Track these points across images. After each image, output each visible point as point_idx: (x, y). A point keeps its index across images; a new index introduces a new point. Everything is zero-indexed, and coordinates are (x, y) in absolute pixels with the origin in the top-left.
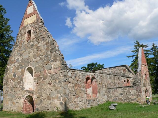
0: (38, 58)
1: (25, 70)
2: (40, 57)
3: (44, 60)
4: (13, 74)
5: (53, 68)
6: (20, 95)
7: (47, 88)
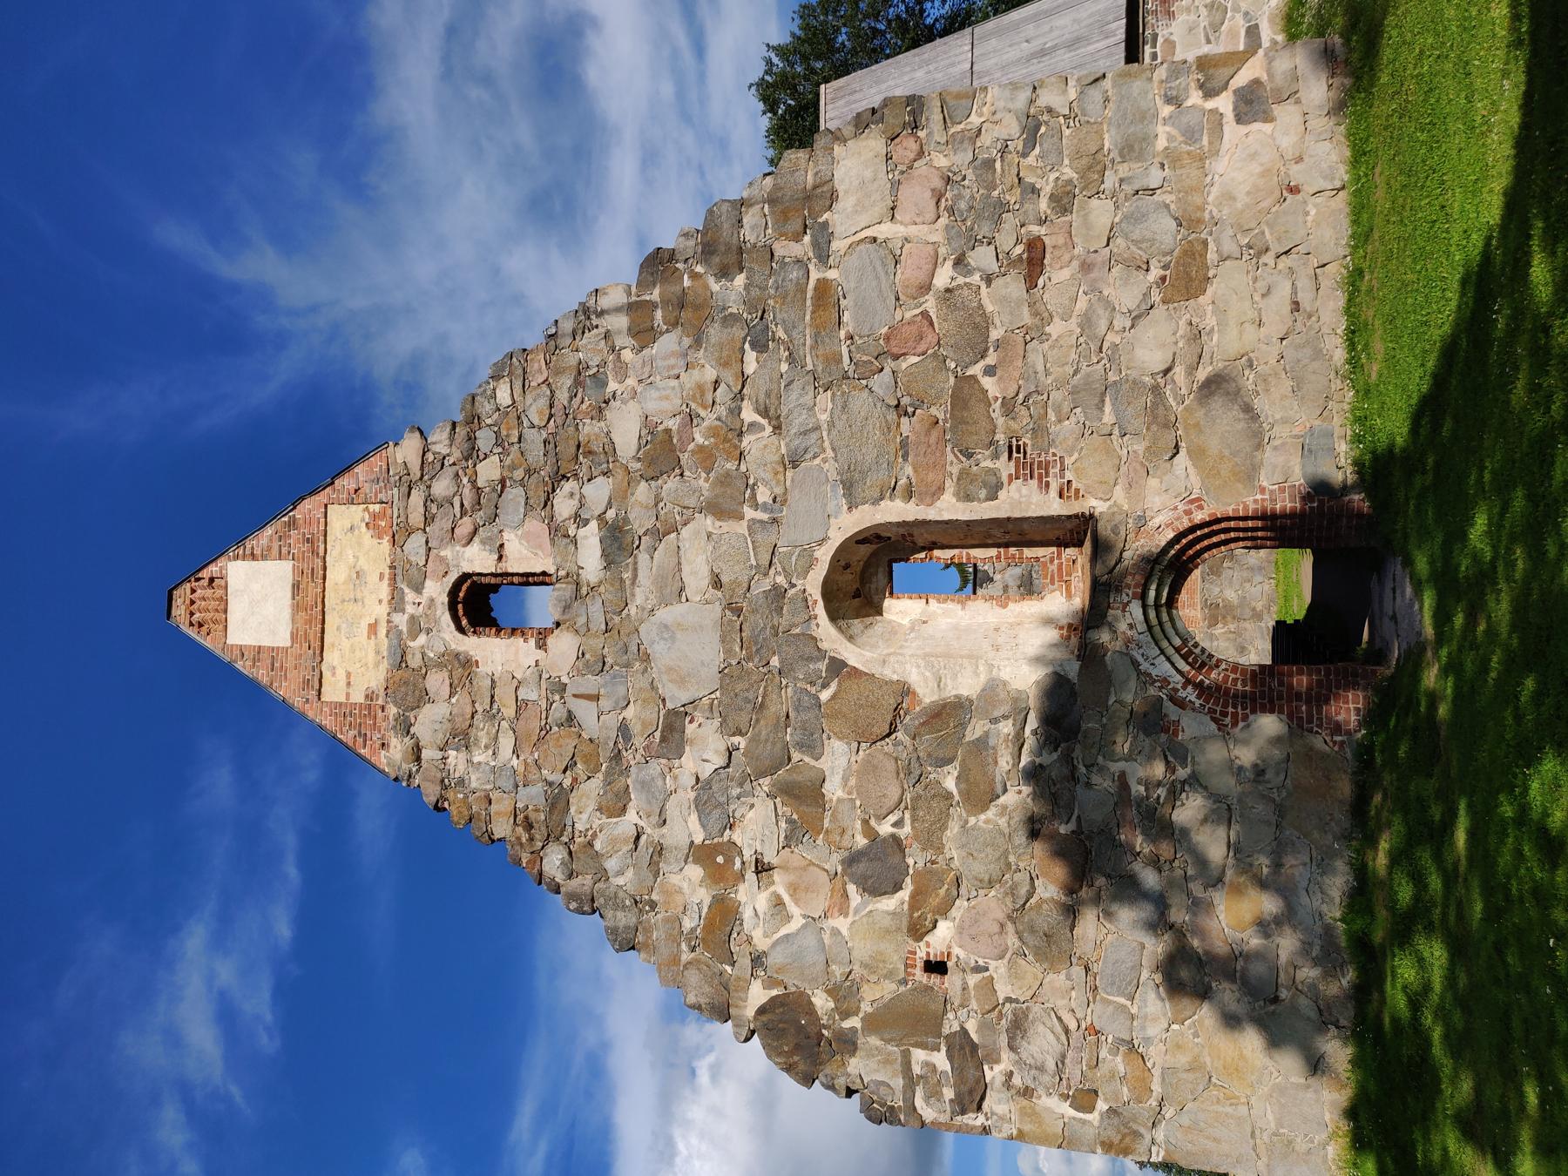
2: (749, 415)
3: (791, 359)
5: (884, 230)
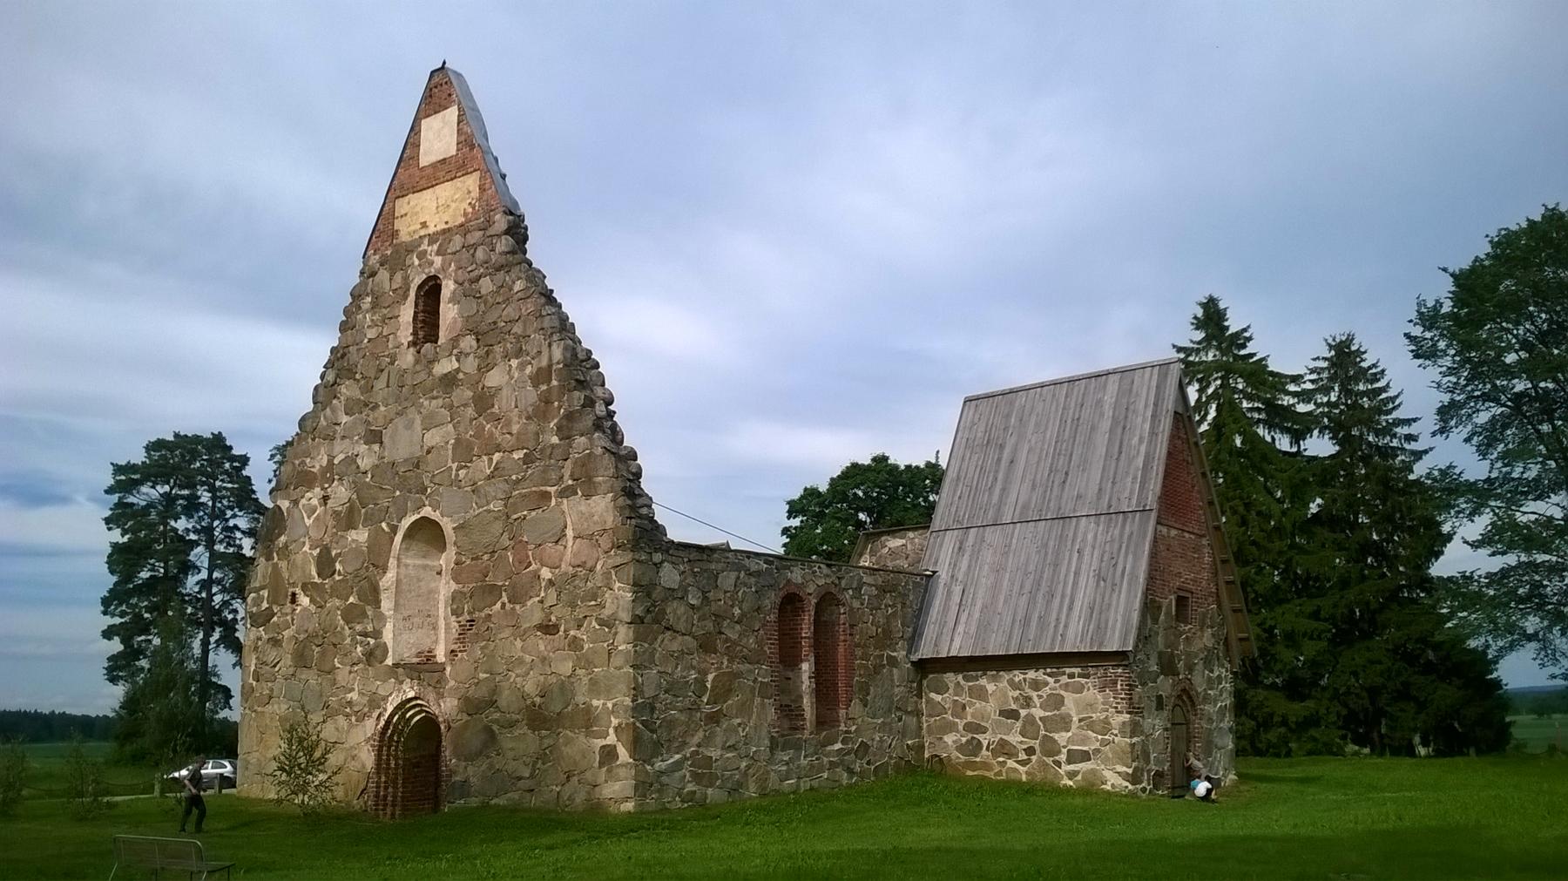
0: (483, 466)
1: (399, 538)
3: (518, 481)
4: (316, 552)
5: (570, 533)
6: (354, 696)
7: (528, 658)
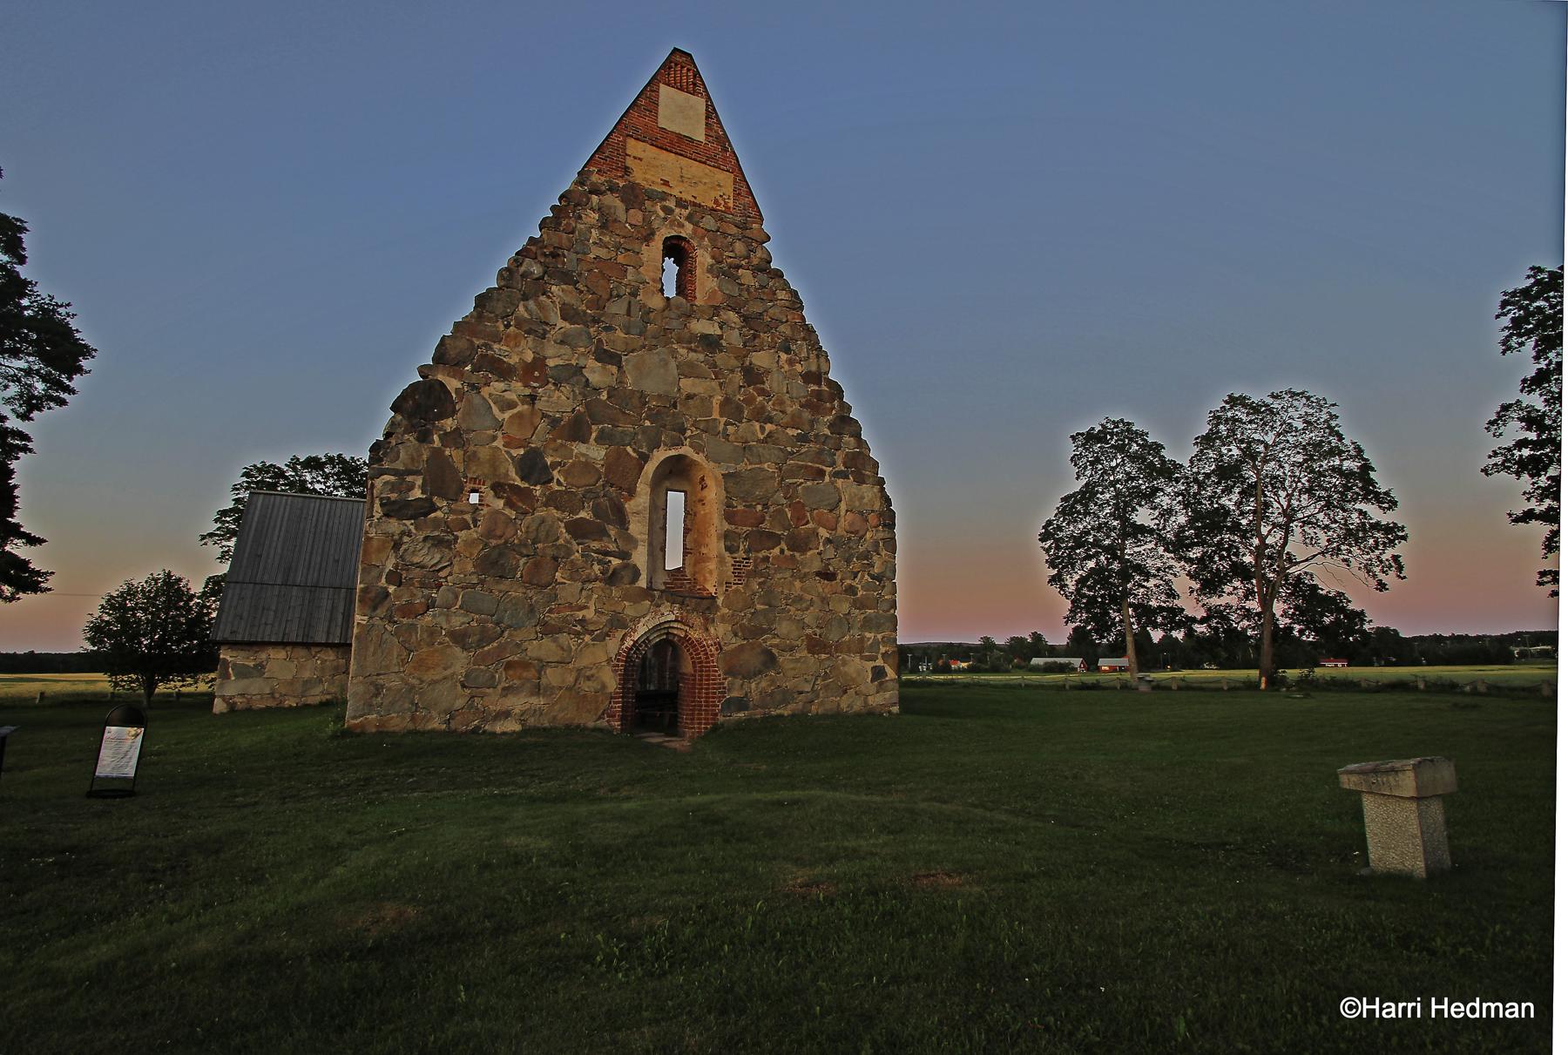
5: (843, 506)
6: (589, 614)
